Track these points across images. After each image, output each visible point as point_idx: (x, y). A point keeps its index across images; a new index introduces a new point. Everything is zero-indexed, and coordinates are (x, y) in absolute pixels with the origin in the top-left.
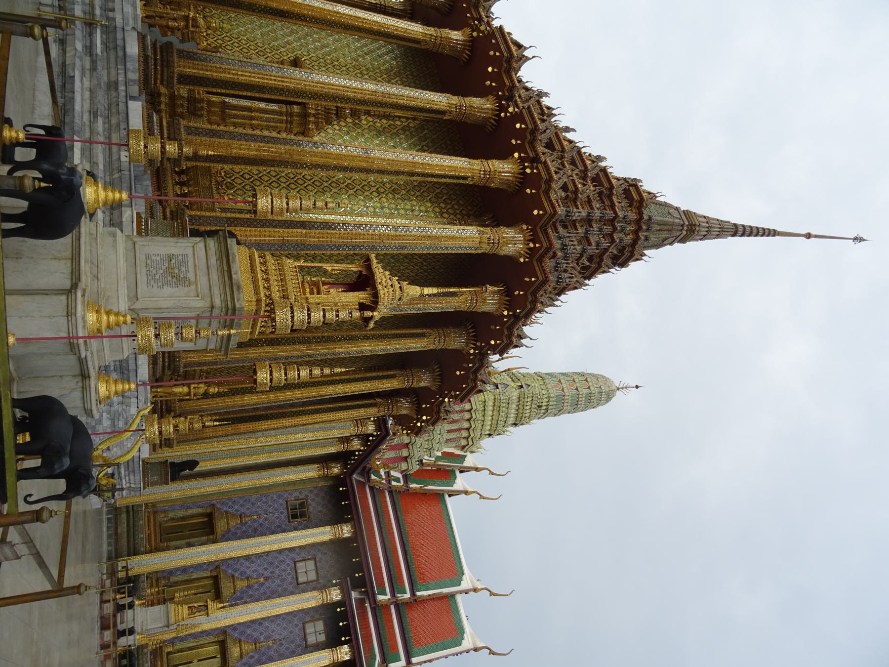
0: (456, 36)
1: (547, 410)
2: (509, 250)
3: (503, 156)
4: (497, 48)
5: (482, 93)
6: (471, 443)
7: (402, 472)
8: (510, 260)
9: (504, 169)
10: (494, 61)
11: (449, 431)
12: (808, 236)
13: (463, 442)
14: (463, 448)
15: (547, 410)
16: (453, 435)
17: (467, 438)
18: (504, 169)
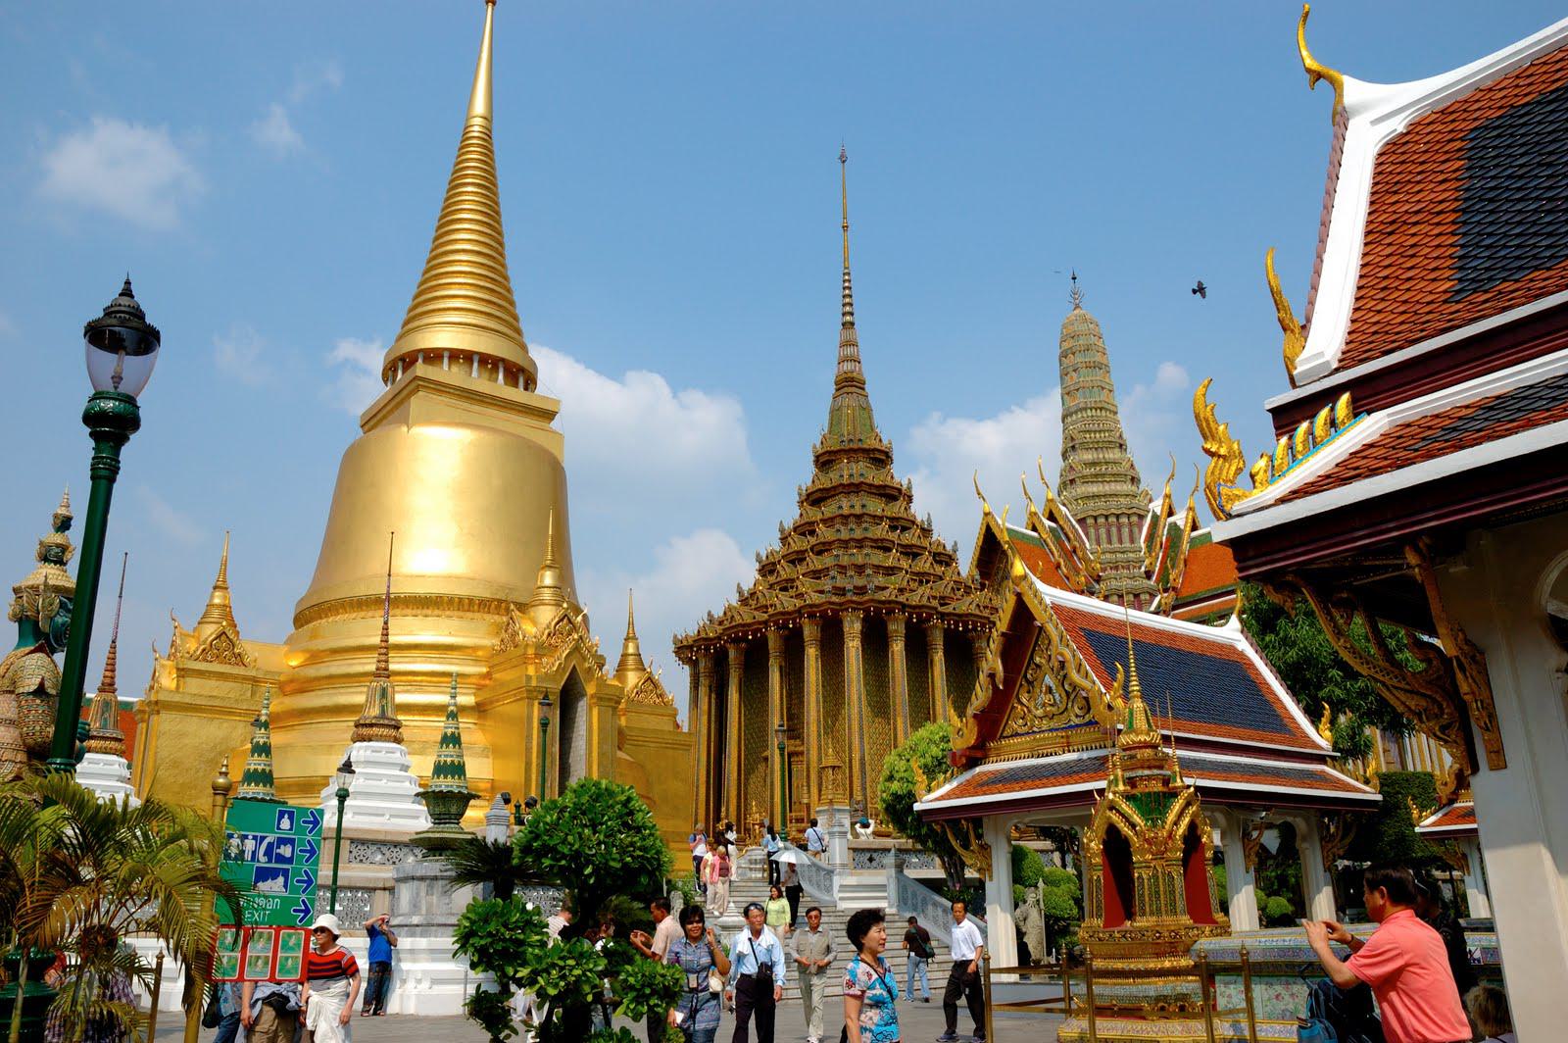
0: (732, 654)
1: (1101, 409)
2: (858, 626)
3: (801, 627)
4: (736, 633)
5: (764, 640)
6: (1134, 510)
7: (1153, 596)
8: (864, 620)
9: (810, 631)
10: (746, 634)
11: (1121, 541)
12: (845, 228)
13: (1134, 519)
14: (1141, 517)
15: (1101, 409)
16: (1125, 531)
17: (1129, 516)
18: (810, 631)
